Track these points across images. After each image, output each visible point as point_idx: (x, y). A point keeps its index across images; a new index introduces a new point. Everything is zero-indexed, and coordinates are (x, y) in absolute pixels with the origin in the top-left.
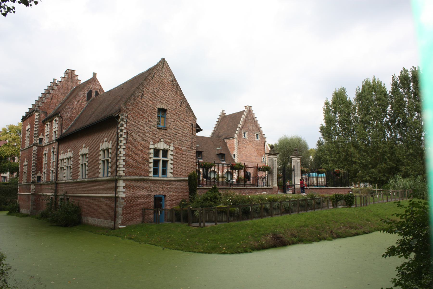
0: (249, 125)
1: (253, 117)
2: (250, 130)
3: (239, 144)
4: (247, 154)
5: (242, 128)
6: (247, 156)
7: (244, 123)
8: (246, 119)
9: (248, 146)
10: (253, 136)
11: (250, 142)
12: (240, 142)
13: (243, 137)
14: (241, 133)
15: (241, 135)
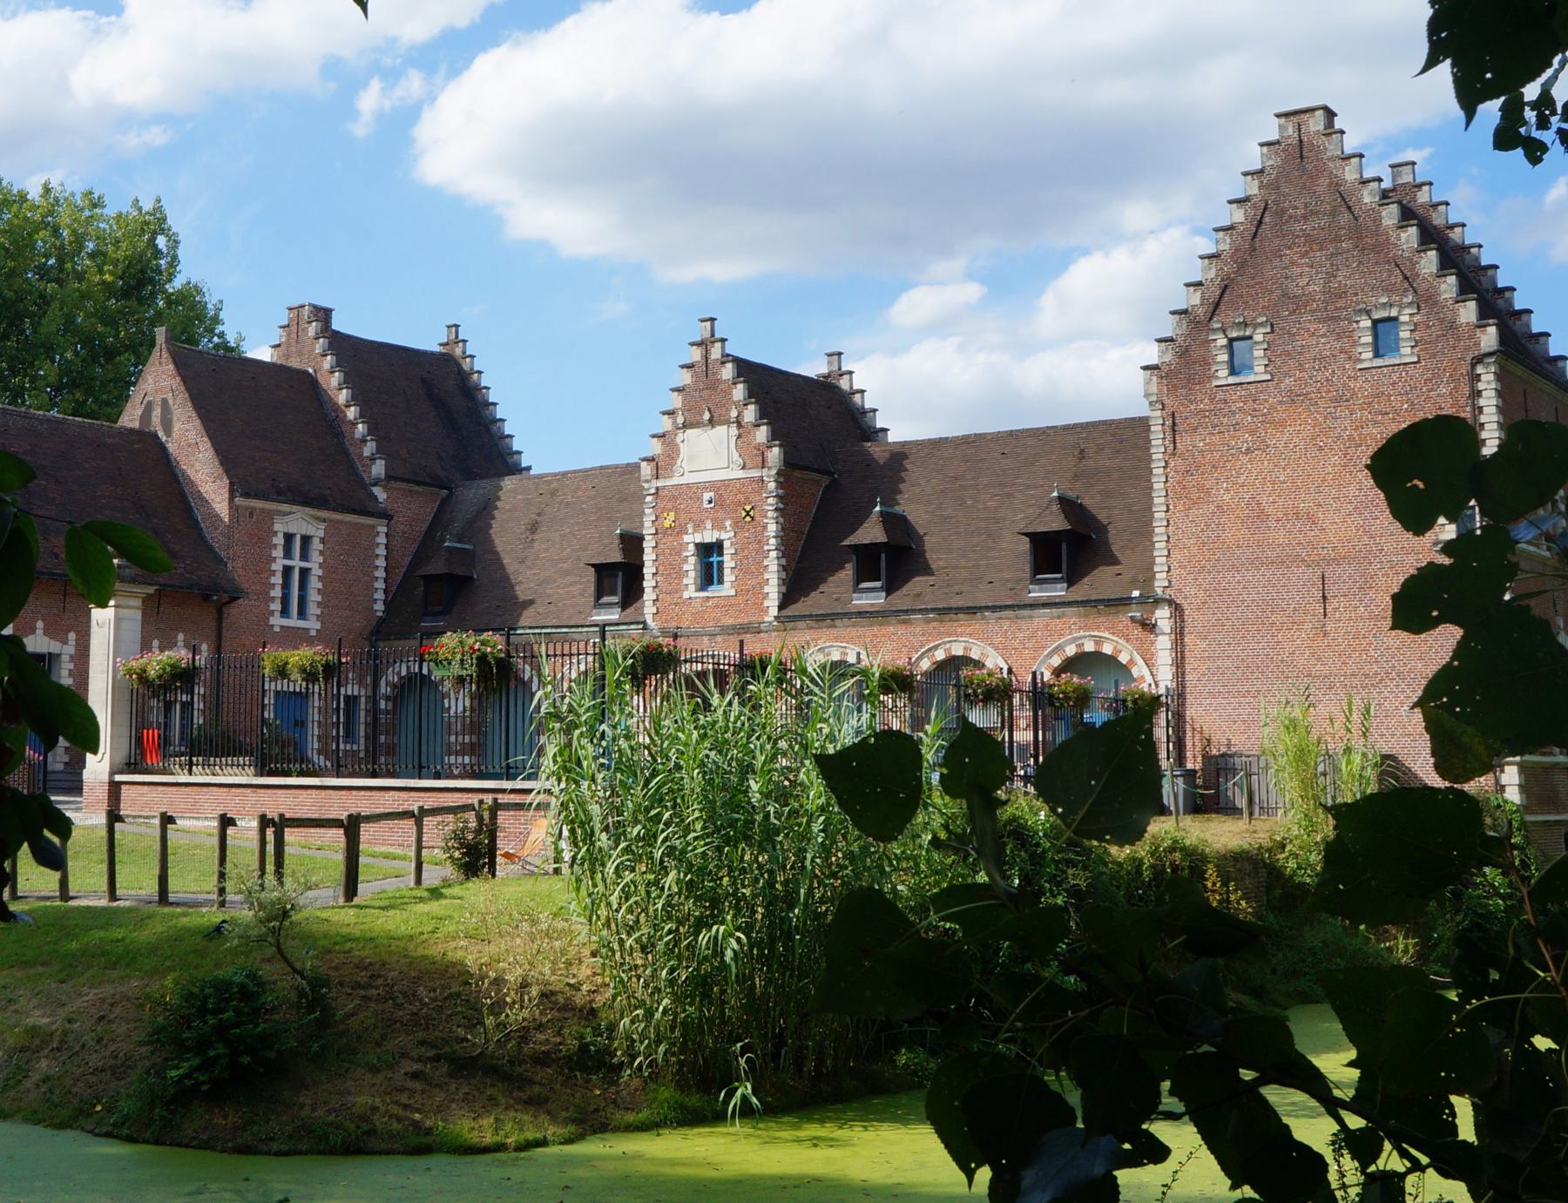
0: (1293, 263)
1: (1336, 185)
2: (1298, 304)
3: (1184, 442)
4: (1264, 500)
5: (1217, 305)
6: (1262, 515)
7: (1242, 265)
8: (1260, 222)
9: (1277, 439)
10: (1326, 345)
11: (1293, 398)
12: (1194, 421)
13: (1223, 373)
14: (1196, 354)
15: (1207, 362)
